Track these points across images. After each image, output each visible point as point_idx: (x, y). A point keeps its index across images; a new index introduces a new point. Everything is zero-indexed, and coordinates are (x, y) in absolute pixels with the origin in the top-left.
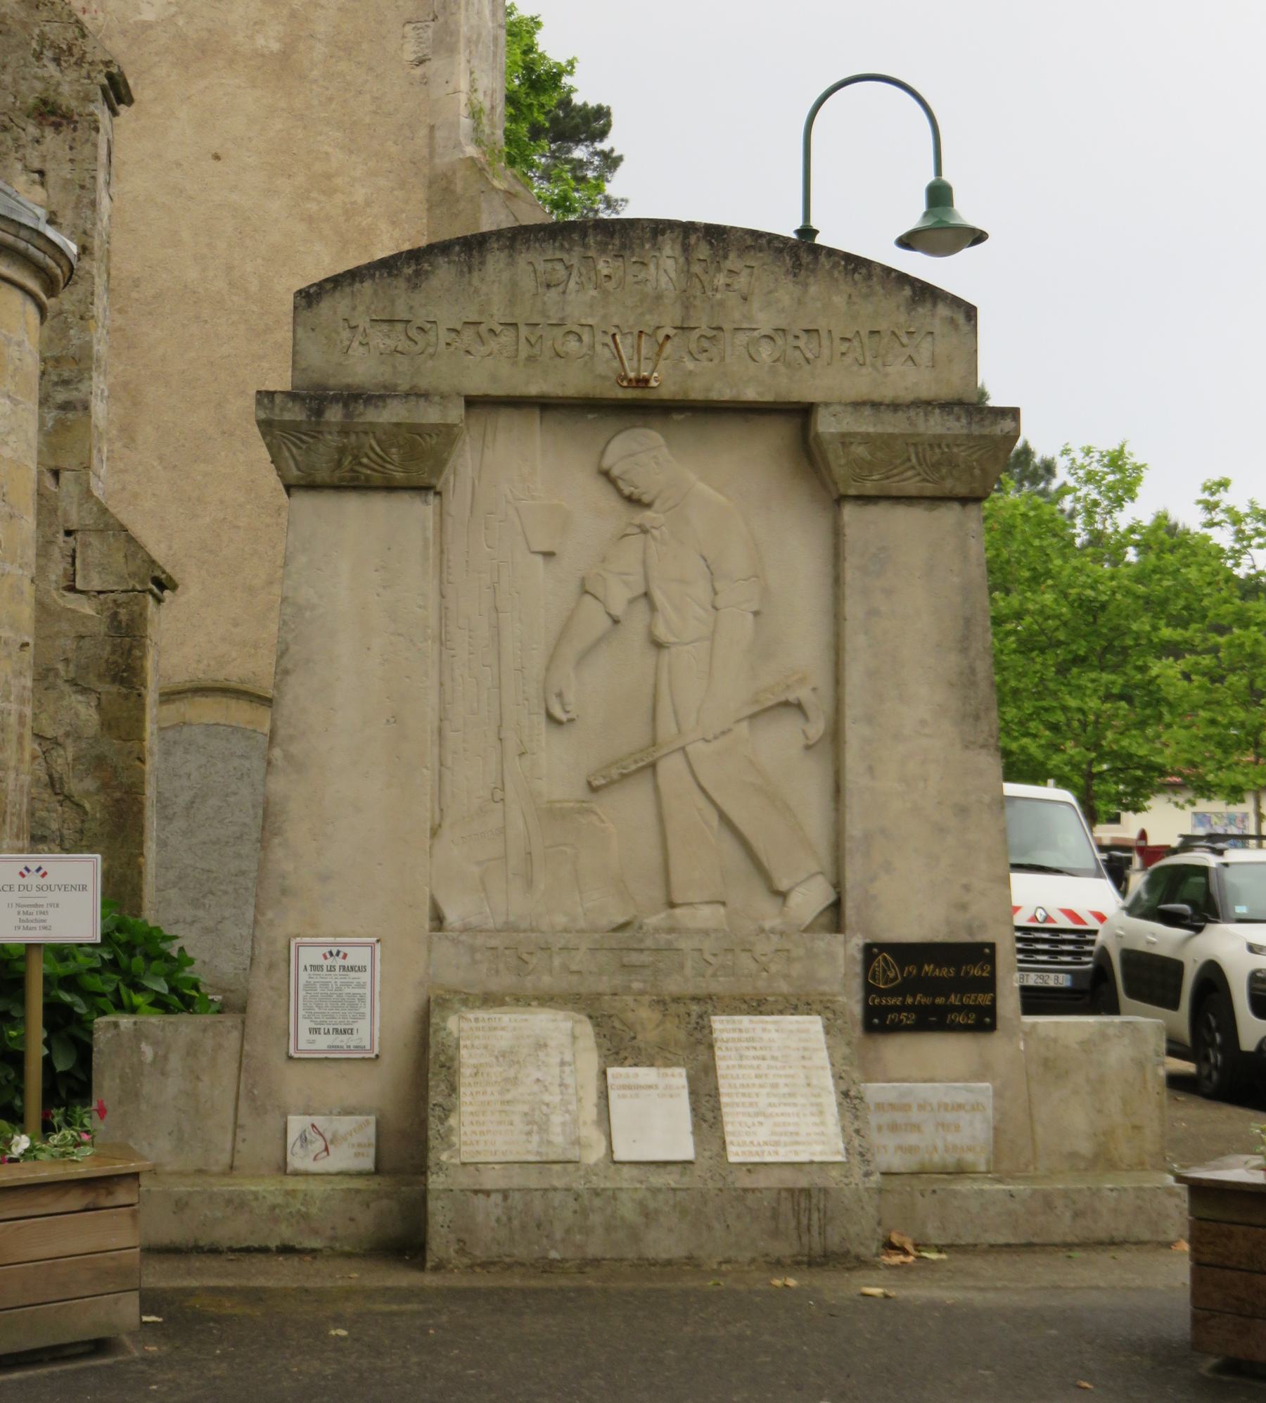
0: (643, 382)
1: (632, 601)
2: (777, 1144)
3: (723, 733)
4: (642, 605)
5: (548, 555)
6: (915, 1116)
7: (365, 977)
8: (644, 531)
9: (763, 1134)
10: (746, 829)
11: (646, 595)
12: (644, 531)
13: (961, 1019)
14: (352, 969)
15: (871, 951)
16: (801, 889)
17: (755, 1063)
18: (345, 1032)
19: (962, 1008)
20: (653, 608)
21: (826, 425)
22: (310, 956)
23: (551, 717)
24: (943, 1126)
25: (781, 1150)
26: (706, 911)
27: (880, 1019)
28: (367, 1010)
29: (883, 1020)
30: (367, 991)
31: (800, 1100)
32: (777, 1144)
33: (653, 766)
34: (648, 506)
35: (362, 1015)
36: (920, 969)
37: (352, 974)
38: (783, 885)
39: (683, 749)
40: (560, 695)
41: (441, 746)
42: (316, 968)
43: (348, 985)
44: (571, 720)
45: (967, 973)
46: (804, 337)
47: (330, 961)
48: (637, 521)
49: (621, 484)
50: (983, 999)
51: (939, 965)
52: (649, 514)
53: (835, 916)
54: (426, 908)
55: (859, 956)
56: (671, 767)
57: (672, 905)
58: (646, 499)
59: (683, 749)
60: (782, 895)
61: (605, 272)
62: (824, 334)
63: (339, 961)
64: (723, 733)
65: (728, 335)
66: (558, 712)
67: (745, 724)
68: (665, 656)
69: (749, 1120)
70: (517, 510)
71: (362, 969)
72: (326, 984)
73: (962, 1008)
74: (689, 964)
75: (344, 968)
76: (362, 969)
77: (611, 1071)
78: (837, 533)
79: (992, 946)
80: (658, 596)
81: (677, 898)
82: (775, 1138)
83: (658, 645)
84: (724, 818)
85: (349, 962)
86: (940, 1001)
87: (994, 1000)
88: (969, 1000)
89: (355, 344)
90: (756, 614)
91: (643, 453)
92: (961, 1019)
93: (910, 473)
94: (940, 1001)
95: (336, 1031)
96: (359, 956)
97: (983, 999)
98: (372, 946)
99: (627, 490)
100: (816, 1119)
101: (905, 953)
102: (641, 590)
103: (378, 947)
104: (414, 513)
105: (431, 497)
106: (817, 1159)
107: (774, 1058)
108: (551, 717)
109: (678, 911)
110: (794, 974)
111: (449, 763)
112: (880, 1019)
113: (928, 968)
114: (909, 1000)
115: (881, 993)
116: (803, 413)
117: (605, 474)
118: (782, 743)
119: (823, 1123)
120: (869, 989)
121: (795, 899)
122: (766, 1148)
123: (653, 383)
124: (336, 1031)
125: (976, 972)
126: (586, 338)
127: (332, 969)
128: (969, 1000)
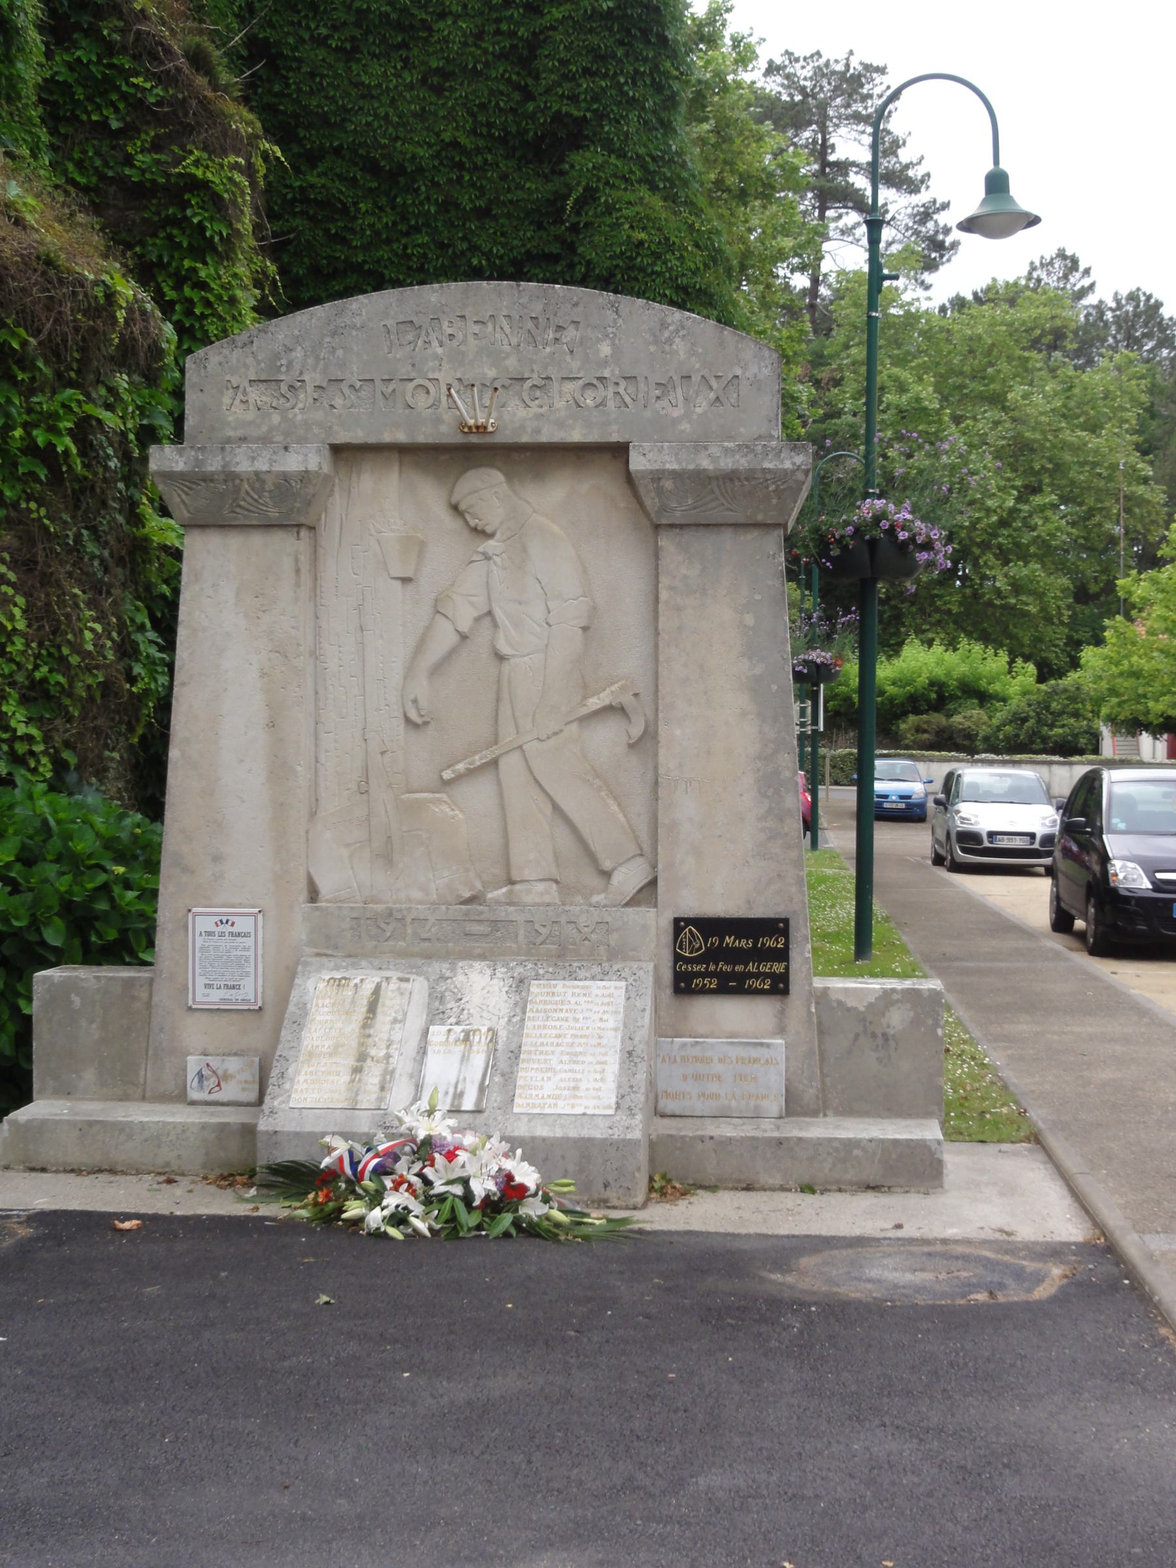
0: (481, 429)
1: (478, 620)
2: (558, 1097)
3: (556, 734)
4: (487, 622)
5: (406, 580)
6: (718, 1068)
7: (249, 942)
8: (488, 558)
9: (549, 1088)
10: (575, 817)
11: (490, 613)
12: (488, 558)
13: (757, 984)
14: (239, 935)
15: (679, 925)
16: (622, 869)
17: (558, 1024)
18: (233, 987)
19: (757, 976)
20: (495, 625)
21: (638, 462)
22: (204, 923)
23: (408, 720)
24: (741, 1077)
25: (561, 1103)
26: (540, 887)
27: (685, 984)
28: (252, 970)
29: (689, 984)
30: (252, 953)
31: (589, 1059)
32: (558, 1097)
33: (494, 763)
34: (491, 536)
35: (247, 974)
36: (722, 941)
37: (239, 939)
38: (607, 865)
39: (520, 747)
40: (415, 701)
41: (316, 745)
42: (209, 934)
43: (236, 948)
44: (426, 723)
45: (763, 944)
46: (623, 384)
47: (221, 928)
48: (481, 549)
49: (467, 516)
50: (778, 968)
51: (739, 937)
52: (491, 542)
53: (649, 891)
54: (303, 884)
55: (670, 930)
56: (511, 765)
57: (512, 882)
58: (489, 529)
59: (520, 747)
60: (607, 875)
61: (450, 331)
62: (641, 379)
63: (227, 928)
64: (556, 734)
65: (556, 385)
66: (413, 716)
67: (575, 725)
68: (506, 667)
69: (540, 1076)
70: (378, 541)
71: (247, 935)
72: (216, 948)
73: (757, 976)
74: (522, 932)
75: (232, 934)
76: (247, 935)
77: (432, 1028)
78: (656, 554)
79: (786, 921)
80: (499, 613)
81: (515, 876)
82: (558, 1092)
83: (500, 658)
84: (556, 807)
85: (235, 929)
86: (739, 968)
87: (787, 968)
88: (765, 968)
89: (237, 402)
90: (585, 629)
91: (487, 490)
92: (757, 984)
93: (713, 504)
94: (739, 968)
95: (226, 986)
96: (243, 924)
97: (778, 968)
98: (255, 915)
99: (473, 523)
100: (598, 1076)
101: (710, 926)
102: (485, 610)
103: (260, 916)
104: (299, 545)
105: (304, 533)
106: (589, 1112)
107: (576, 1020)
108: (408, 720)
109: (518, 887)
110: (612, 943)
111: (323, 760)
112: (685, 984)
113: (728, 940)
114: (712, 968)
115: (688, 961)
116: (620, 451)
117: (455, 508)
118: (607, 739)
119: (602, 1080)
120: (677, 958)
121: (617, 878)
122: (548, 1101)
123: (490, 429)
124: (226, 986)
125: (770, 943)
126: (432, 390)
127: (222, 934)
128: (765, 968)
